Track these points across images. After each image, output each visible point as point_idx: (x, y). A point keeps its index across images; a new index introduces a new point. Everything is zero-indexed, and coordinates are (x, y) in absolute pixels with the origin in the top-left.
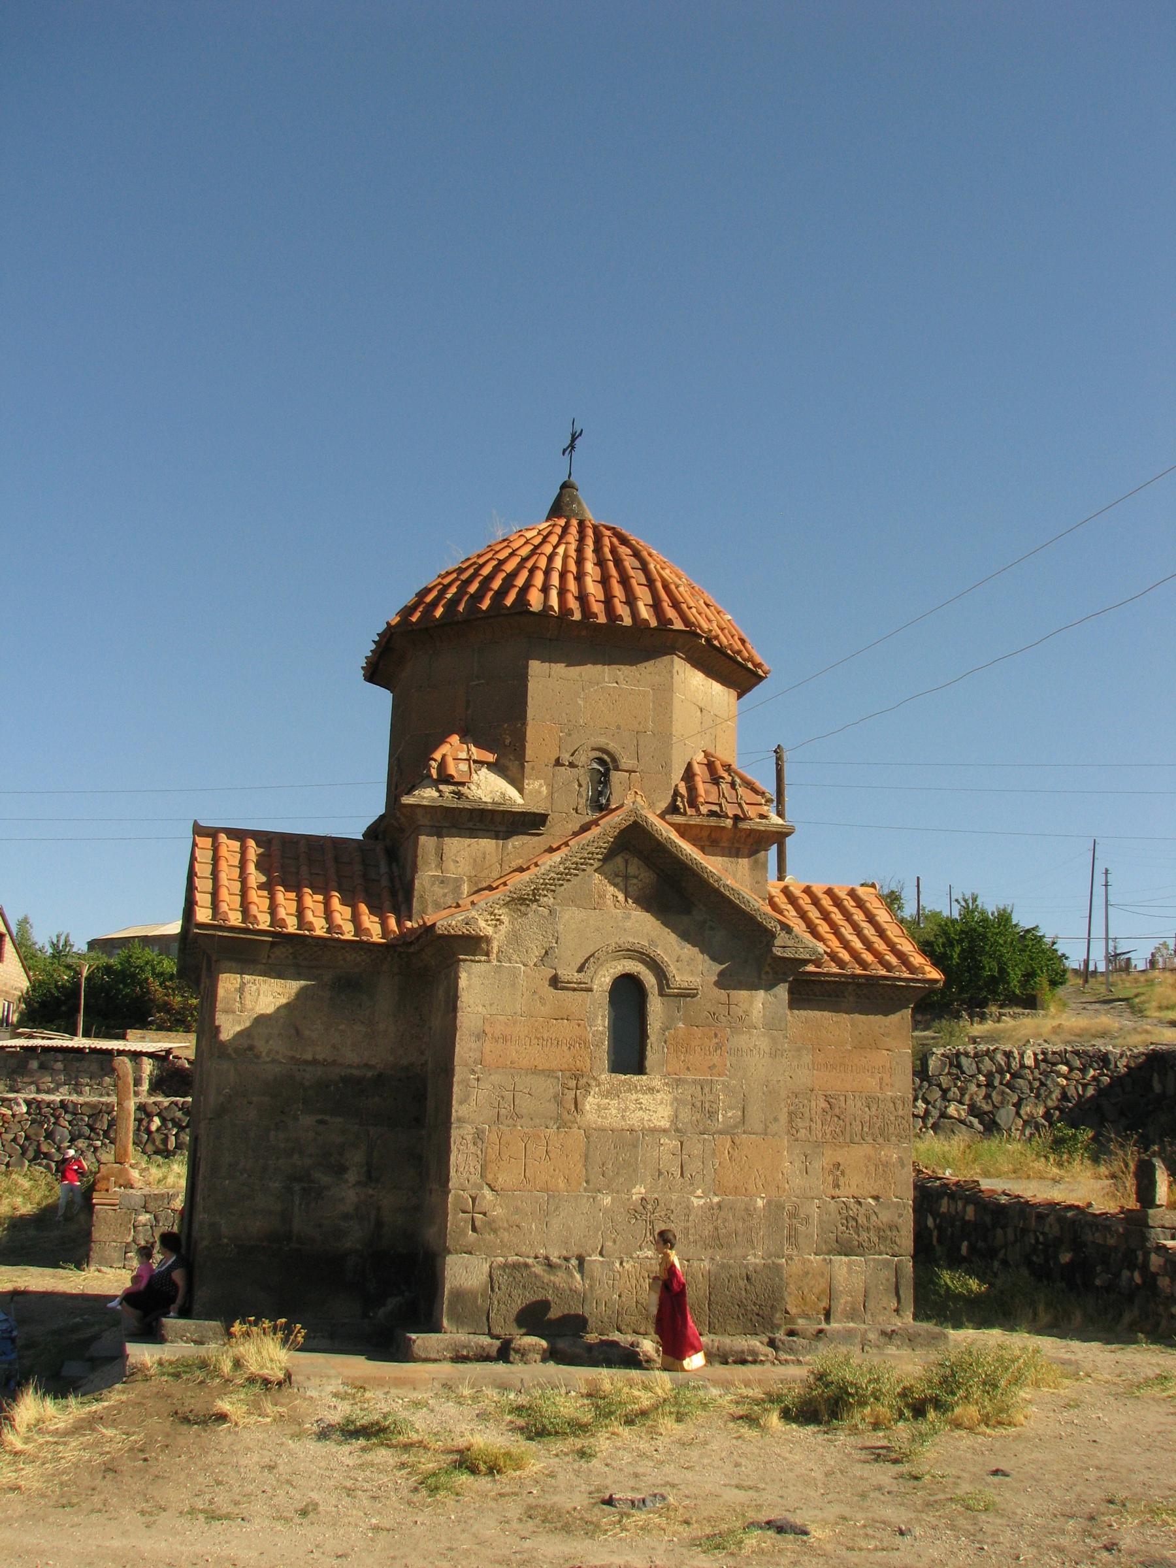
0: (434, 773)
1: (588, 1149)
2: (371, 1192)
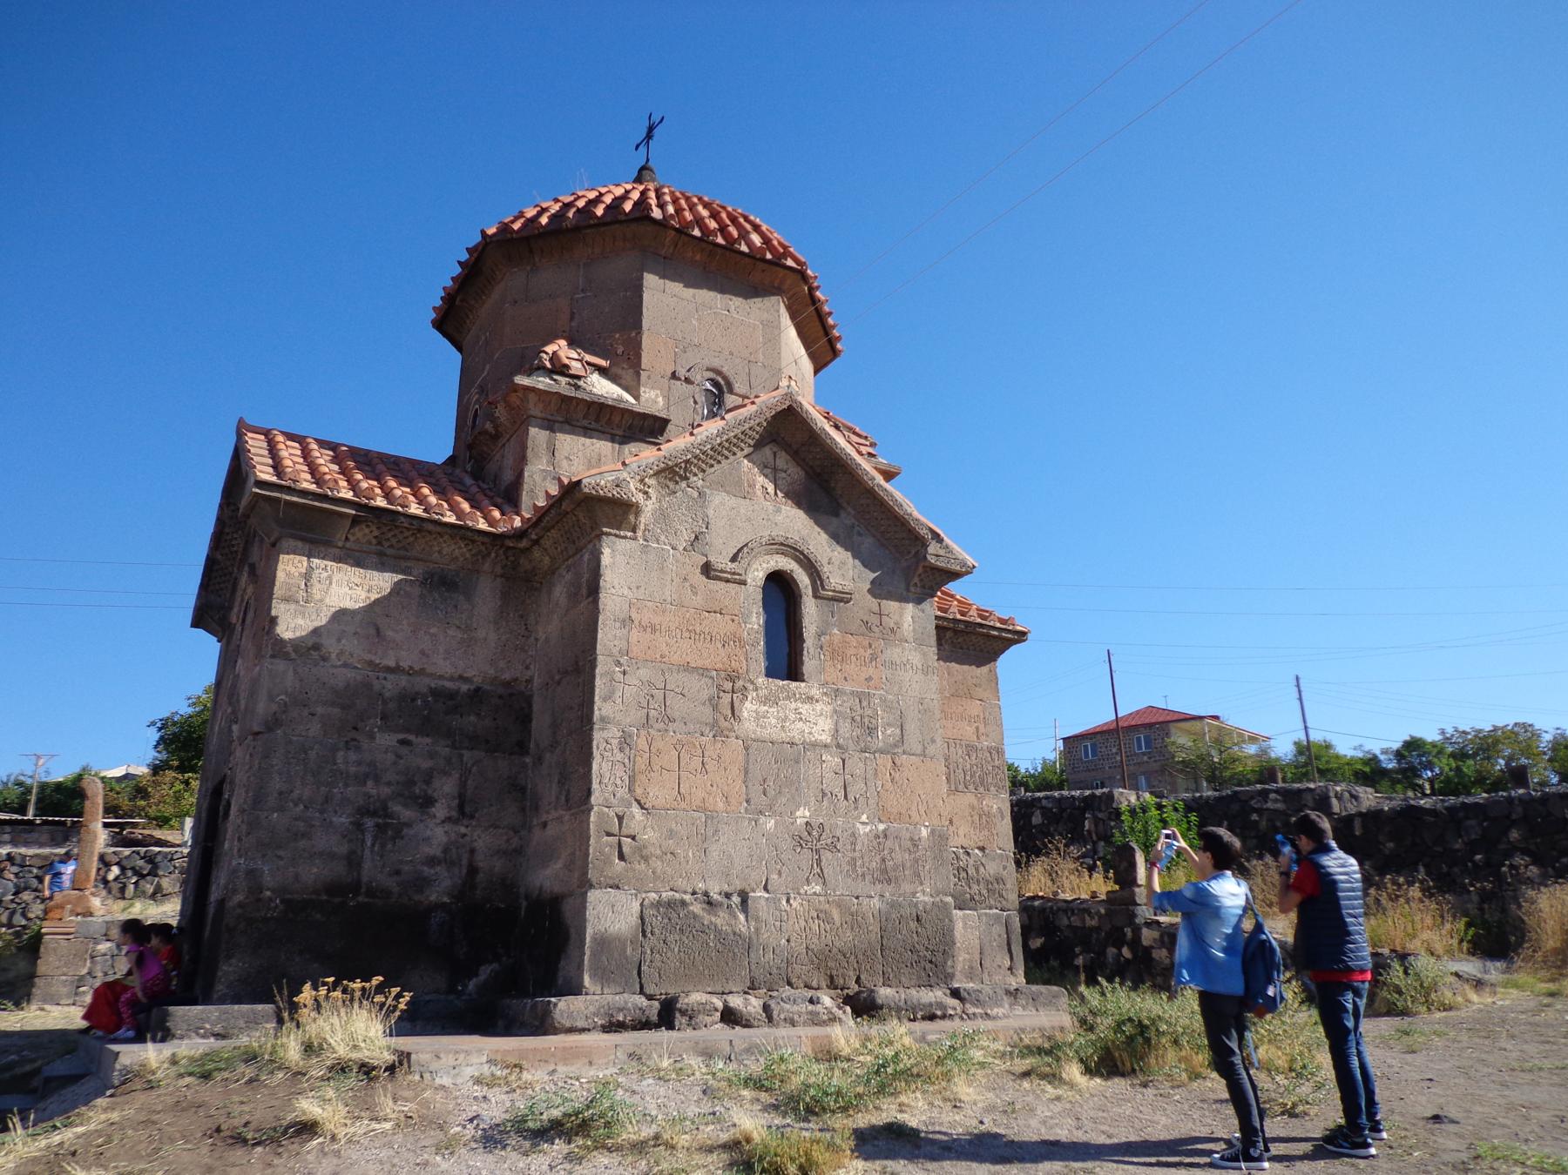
0: (548, 365)
1: (747, 762)
2: (463, 830)
